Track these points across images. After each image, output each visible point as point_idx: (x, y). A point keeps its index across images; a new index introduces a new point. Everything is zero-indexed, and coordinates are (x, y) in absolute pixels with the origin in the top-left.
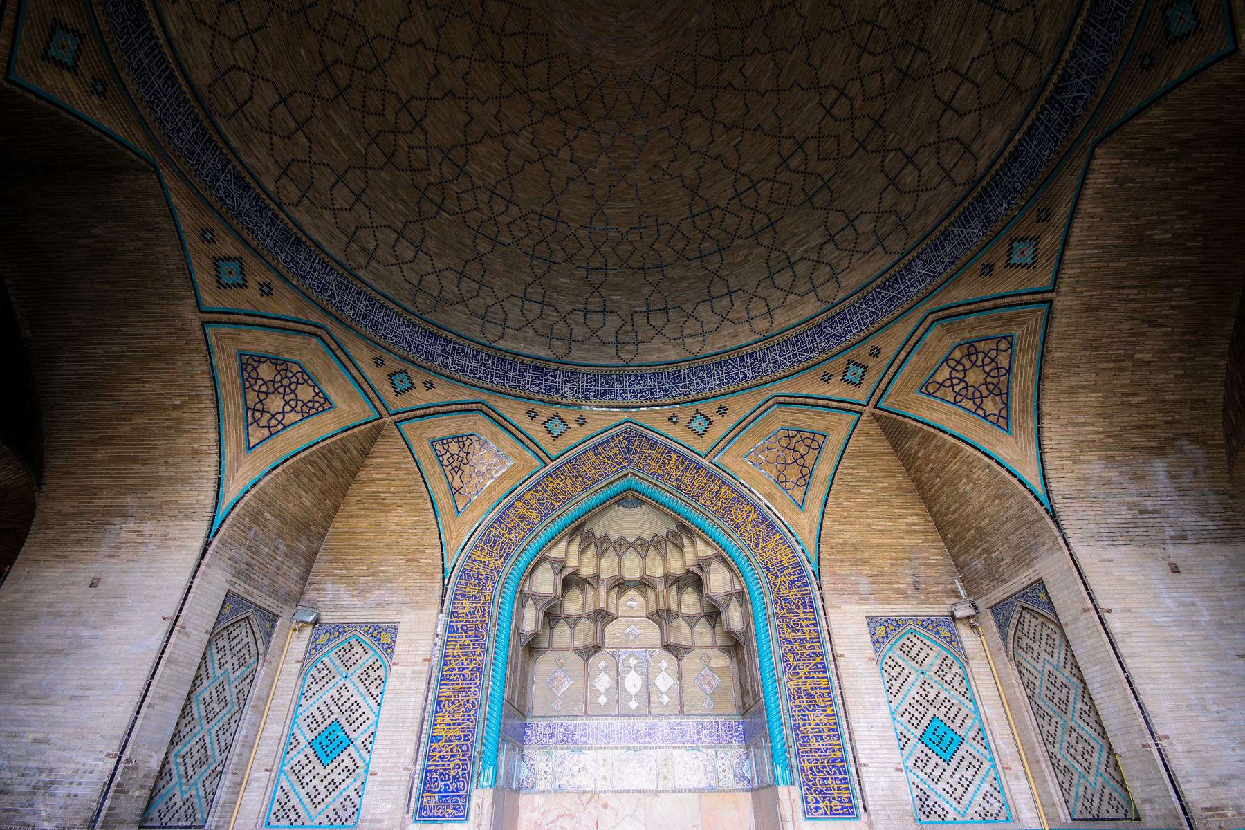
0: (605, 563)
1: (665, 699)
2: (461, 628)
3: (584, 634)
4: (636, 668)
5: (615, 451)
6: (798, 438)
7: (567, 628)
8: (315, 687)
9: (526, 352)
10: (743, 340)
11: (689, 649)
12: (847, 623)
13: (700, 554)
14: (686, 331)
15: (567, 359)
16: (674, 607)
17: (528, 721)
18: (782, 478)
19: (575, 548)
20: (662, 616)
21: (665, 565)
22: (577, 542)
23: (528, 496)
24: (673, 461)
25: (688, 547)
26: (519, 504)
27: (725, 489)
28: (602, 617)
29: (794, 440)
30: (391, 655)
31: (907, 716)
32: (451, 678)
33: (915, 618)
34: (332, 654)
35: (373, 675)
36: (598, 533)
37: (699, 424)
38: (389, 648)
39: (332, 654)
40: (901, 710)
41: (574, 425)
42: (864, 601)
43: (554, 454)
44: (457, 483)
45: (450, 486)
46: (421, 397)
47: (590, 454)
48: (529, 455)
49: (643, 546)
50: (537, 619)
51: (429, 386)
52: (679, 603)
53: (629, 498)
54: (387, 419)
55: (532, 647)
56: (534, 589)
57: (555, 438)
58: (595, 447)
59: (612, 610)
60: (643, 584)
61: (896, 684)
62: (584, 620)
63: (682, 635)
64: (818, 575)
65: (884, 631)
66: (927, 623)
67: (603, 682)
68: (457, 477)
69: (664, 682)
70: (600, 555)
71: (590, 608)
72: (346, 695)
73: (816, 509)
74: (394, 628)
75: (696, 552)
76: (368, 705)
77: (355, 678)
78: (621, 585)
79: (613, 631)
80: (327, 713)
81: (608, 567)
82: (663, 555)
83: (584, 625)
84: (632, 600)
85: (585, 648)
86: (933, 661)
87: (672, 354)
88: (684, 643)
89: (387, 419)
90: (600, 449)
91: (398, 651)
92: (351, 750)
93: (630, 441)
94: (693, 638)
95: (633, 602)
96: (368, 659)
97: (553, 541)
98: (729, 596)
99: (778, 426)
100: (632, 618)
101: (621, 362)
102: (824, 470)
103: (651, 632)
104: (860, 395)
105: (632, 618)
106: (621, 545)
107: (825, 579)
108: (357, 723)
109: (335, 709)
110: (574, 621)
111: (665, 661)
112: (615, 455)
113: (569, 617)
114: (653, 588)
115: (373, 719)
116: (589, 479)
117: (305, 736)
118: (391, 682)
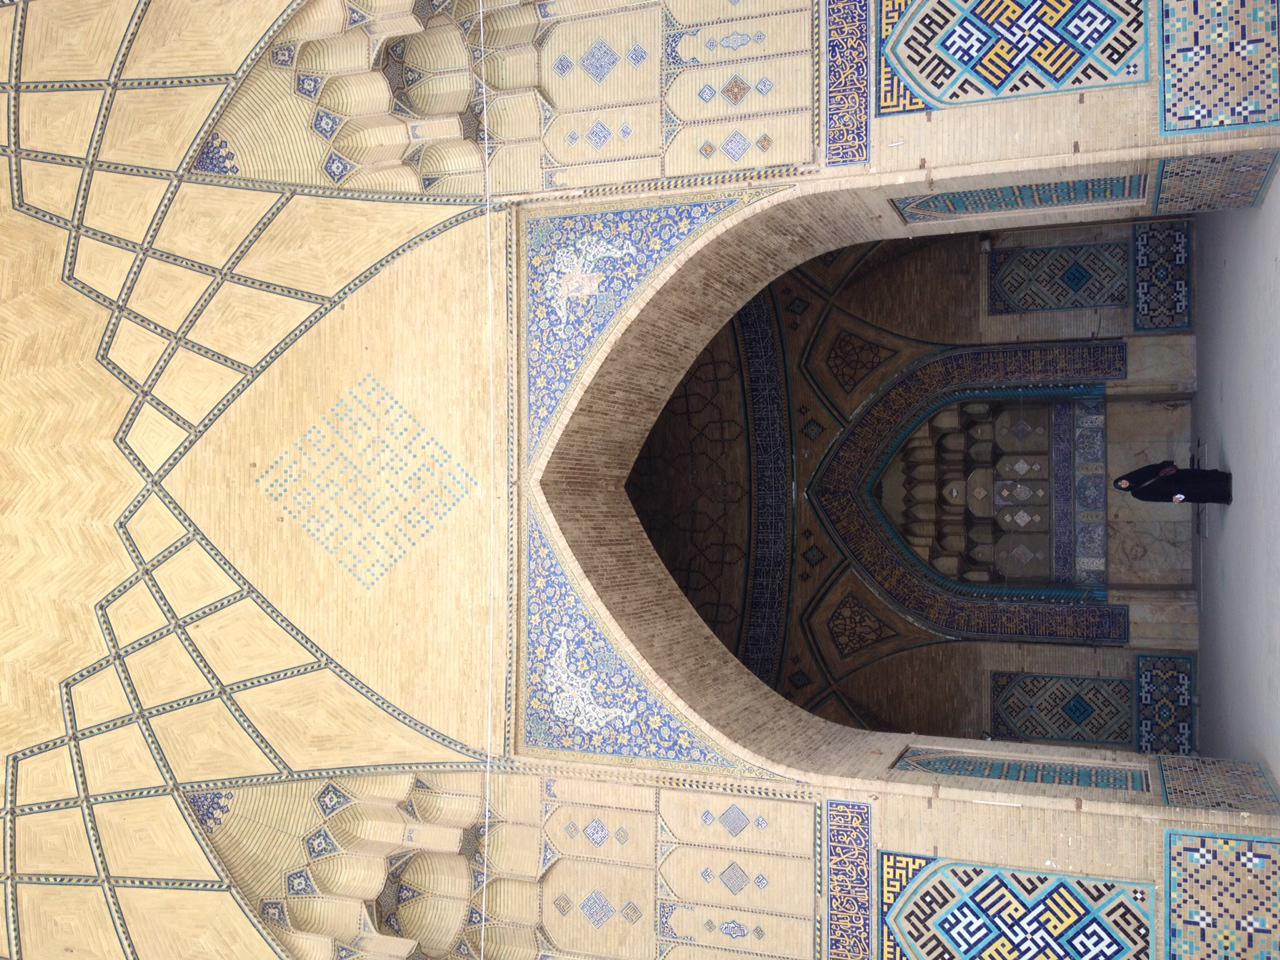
0: (922, 515)
1: (1036, 467)
2: (992, 631)
3: (982, 535)
4: (1011, 489)
5: (836, 504)
6: (838, 351)
7: (979, 549)
8: (1040, 729)
9: (741, 584)
10: (737, 388)
11: (995, 447)
12: (994, 329)
13: (927, 435)
14: (717, 436)
15: (744, 548)
16: (960, 457)
17: (1053, 578)
18: (869, 365)
19: (916, 541)
20: (969, 465)
21: (926, 463)
22: (910, 538)
23: (880, 578)
24: (847, 455)
25: (916, 443)
26: (887, 585)
27: (874, 412)
28: (969, 520)
29: (839, 353)
30: (1017, 674)
31: (1061, 298)
32: (1027, 636)
33: (991, 279)
34: (1015, 721)
35: (1030, 686)
36: (900, 520)
37: (814, 431)
38: (1011, 677)
39: (1015, 721)
40: (1056, 301)
41: (812, 540)
42: (976, 315)
43: (839, 556)
44: (873, 636)
45: (877, 641)
46: (807, 662)
47: (839, 526)
48: (843, 579)
49: (910, 483)
50: (979, 570)
51: (796, 660)
52: (956, 452)
53: (877, 492)
54: (835, 687)
55: (997, 578)
56: (955, 572)
57: (825, 557)
58: (832, 522)
59: (962, 510)
60: (941, 484)
61: (1038, 301)
62: (971, 535)
63: (983, 450)
64: (955, 347)
65: (1000, 305)
66: (994, 270)
67: (1022, 518)
68: (868, 636)
69: (1022, 467)
70: (917, 520)
71: (960, 529)
72: (1045, 704)
73: (900, 343)
74: (996, 676)
75: (925, 438)
76: (1053, 687)
77: (1032, 701)
78: (941, 501)
79: (978, 511)
80: (1057, 716)
81: (924, 513)
82: (916, 464)
83: (973, 536)
84: (951, 492)
85: (993, 533)
86: (1022, 271)
87: (739, 451)
88: (990, 449)
89: (835, 687)
90: (833, 518)
91: (1013, 669)
92: (1082, 694)
93: (827, 490)
94: (986, 441)
95: (954, 492)
96: (1018, 693)
97: (915, 555)
98: (962, 413)
99: (823, 365)
100: (974, 492)
101: (745, 500)
102: (870, 334)
103: (978, 476)
104: (818, 304)
105: (974, 492)
106: (909, 500)
107: (958, 342)
108: (1065, 692)
109: (1055, 711)
110: (971, 544)
111: (1004, 466)
112: (840, 504)
113: (966, 546)
114: (945, 473)
115: (1062, 682)
116: (863, 527)
117: (1074, 729)
118: (1036, 670)
